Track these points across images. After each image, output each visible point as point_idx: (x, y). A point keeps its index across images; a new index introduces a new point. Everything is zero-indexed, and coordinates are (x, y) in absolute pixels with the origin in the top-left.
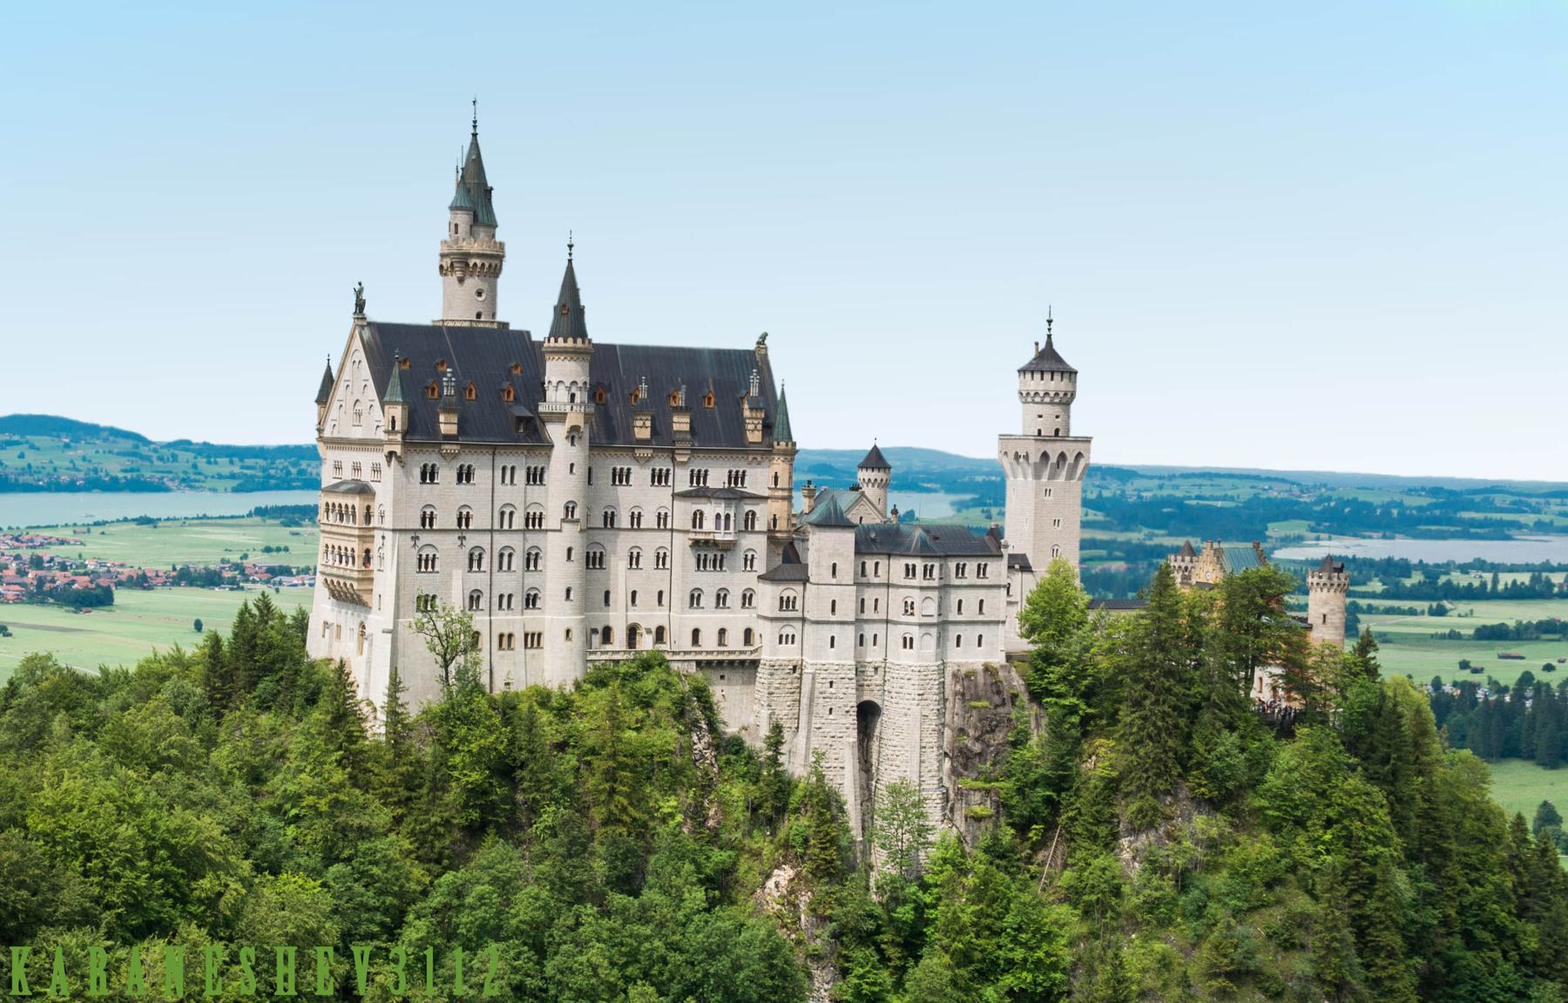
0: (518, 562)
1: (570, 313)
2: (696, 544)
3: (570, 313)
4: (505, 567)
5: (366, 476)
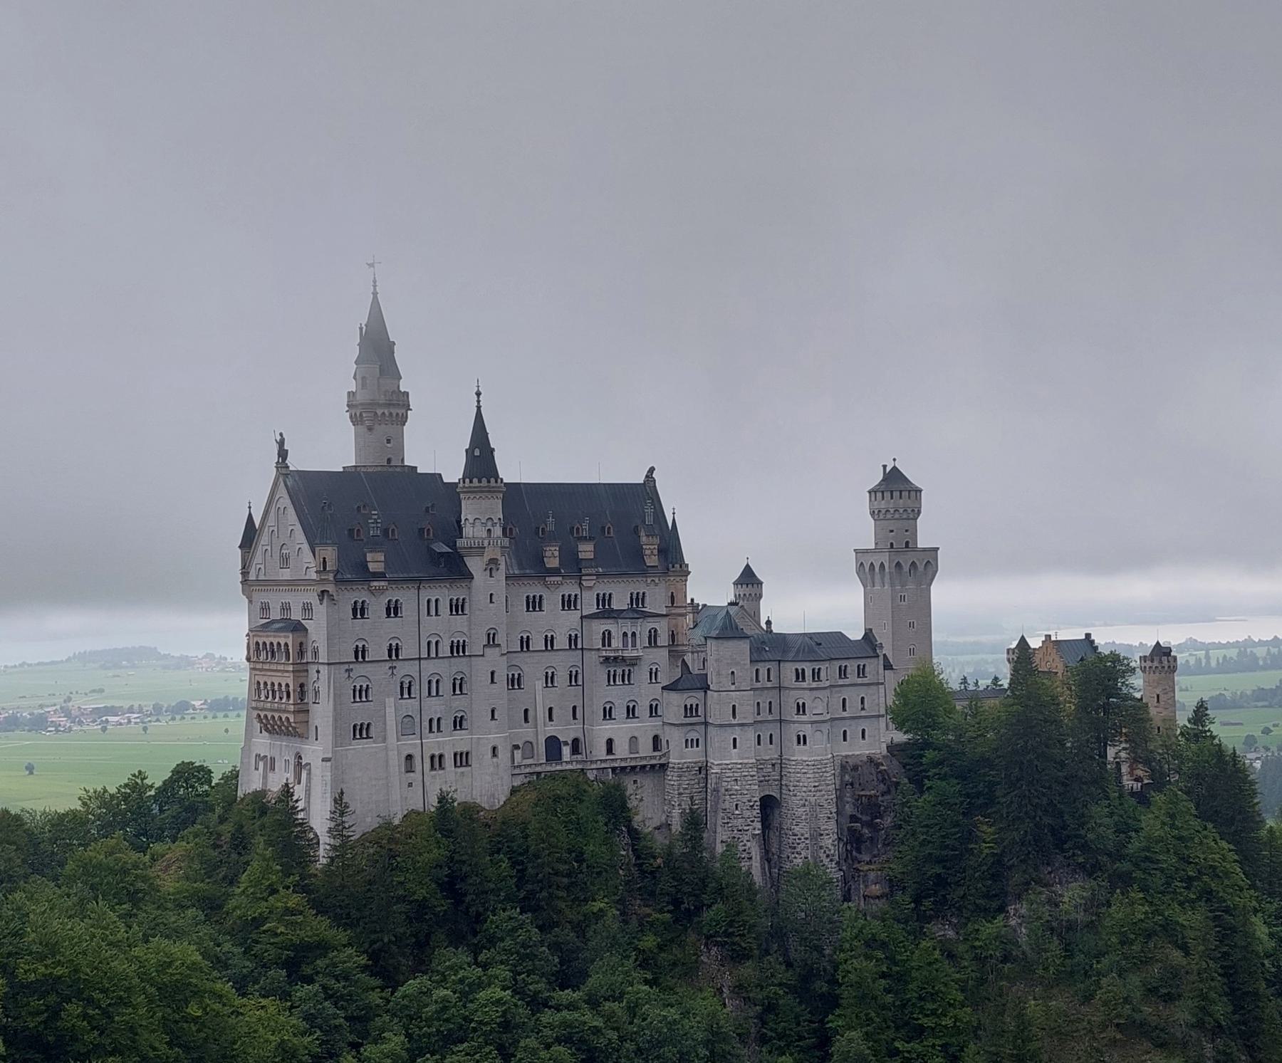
0: (446, 687)
1: (481, 456)
3: (481, 456)
4: (434, 693)
5: (296, 615)
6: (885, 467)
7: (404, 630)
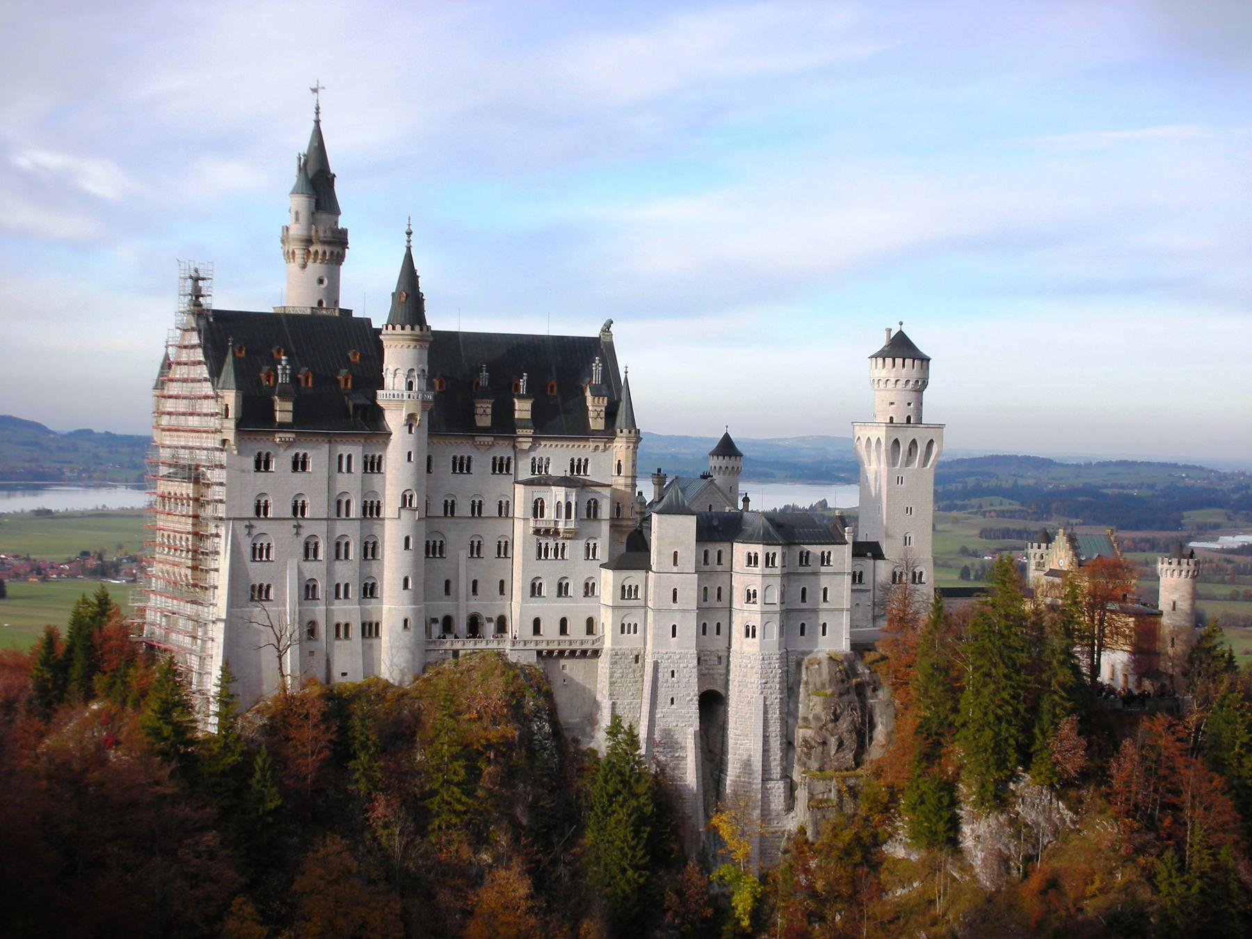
1: (410, 301)
2: (537, 531)
3: (410, 301)
4: (342, 556)
6: (890, 330)
7: (313, 487)
